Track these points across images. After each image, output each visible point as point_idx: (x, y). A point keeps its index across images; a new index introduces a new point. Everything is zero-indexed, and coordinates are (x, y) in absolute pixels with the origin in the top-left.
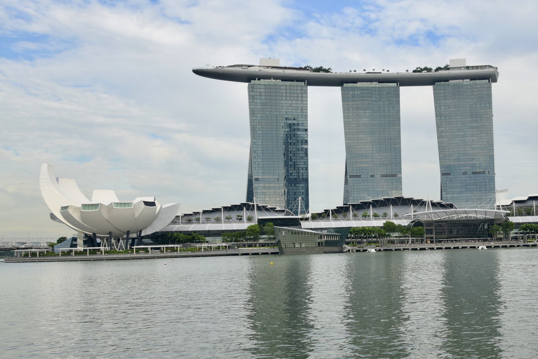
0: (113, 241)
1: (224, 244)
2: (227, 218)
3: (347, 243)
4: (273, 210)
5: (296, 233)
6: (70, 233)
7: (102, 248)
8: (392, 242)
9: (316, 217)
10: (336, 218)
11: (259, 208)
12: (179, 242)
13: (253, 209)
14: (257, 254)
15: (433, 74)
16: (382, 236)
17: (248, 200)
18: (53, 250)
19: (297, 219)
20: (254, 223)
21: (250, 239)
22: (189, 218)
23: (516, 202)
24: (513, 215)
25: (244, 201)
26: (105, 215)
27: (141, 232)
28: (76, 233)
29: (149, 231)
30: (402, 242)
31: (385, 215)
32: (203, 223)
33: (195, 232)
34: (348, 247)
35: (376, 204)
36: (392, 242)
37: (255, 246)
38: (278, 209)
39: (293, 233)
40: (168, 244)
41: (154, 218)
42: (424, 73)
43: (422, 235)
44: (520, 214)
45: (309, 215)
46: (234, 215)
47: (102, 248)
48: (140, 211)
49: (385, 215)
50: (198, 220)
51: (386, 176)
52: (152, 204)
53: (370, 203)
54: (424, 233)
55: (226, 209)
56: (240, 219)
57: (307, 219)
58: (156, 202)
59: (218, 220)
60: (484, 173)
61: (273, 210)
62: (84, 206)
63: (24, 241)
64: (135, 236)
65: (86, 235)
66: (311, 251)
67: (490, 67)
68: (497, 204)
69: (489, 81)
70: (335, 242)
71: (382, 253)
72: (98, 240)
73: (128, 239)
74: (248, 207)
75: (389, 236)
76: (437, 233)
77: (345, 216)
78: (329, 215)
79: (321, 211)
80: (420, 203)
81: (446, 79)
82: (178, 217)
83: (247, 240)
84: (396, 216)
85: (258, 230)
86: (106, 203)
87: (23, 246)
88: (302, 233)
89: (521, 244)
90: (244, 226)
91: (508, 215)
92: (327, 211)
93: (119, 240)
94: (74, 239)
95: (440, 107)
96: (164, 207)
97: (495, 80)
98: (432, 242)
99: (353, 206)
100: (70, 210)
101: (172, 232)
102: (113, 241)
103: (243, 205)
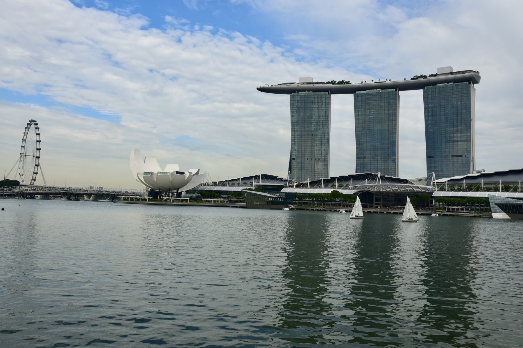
51: (385, 158)
69: (470, 83)
95: (428, 105)
97: (477, 83)
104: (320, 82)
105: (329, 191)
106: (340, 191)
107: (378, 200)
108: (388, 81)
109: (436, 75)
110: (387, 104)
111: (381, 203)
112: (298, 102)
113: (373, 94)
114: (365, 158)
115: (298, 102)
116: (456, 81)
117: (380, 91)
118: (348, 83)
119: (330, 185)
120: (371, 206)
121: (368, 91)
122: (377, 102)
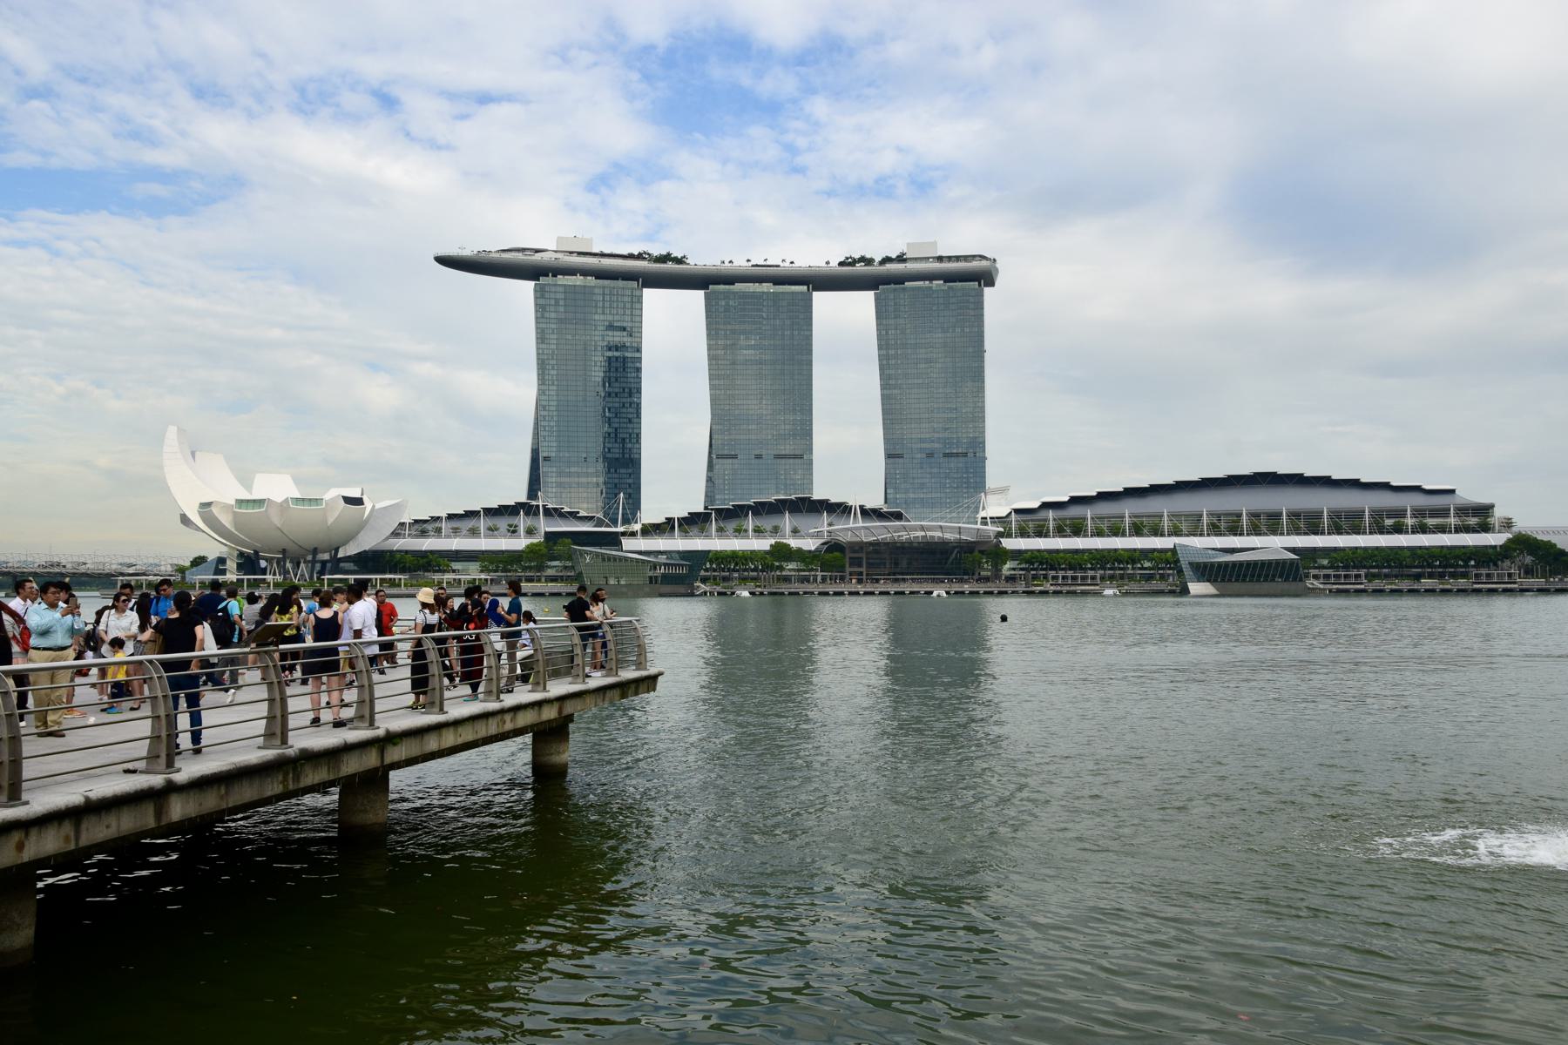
0: (289, 565)
1: (483, 576)
2: (490, 529)
3: (704, 580)
4: (574, 515)
5: (610, 558)
6: (213, 548)
7: (269, 577)
8: (787, 579)
9: (648, 530)
10: (685, 533)
11: (548, 512)
12: (403, 571)
13: (536, 514)
14: (541, 595)
15: (875, 269)
16: (768, 567)
17: (529, 497)
18: (183, 578)
19: (616, 533)
20: (538, 539)
21: (530, 568)
22: (422, 527)
23: (1017, 511)
24: (1009, 536)
25: (523, 498)
26: (276, 520)
27: (337, 550)
28: (225, 549)
29: (351, 550)
30: (805, 580)
31: (776, 530)
32: (447, 537)
33: (432, 552)
34: (703, 587)
35: (761, 509)
36: (787, 579)
37: (539, 581)
38: (583, 513)
39: (605, 558)
40: (384, 572)
41: (362, 525)
42: (860, 267)
43: (842, 568)
44: (1023, 533)
45: (637, 527)
46: (503, 523)
47: (269, 577)
48: (336, 514)
49: (776, 530)
50: (439, 530)
52: (358, 502)
53: (749, 507)
54: (847, 564)
55: (489, 512)
56: (513, 531)
57: (633, 534)
58: (365, 499)
59: (474, 532)
60: (965, 454)
61: (574, 515)
62: (240, 502)
63: (132, 561)
64: (326, 556)
65: (241, 554)
66: (636, 592)
67: (983, 257)
68: (982, 514)
70: (680, 577)
71: (768, 599)
72: (263, 564)
73: (314, 561)
74: (528, 509)
75: (781, 568)
76: (869, 565)
77: (702, 530)
78: (673, 528)
79: (660, 519)
80: (841, 509)
81: (899, 279)
82: (402, 524)
83: (524, 569)
84: (795, 532)
85: (545, 551)
86: (278, 497)
87: (131, 571)
88: (626, 559)
89: (1020, 589)
90: (520, 543)
91: (1000, 535)
92: (670, 520)
93: (298, 564)
94: (221, 561)
96: (378, 506)
98: (860, 581)
99: (718, 511)
100: (214, 509)
101: (392, 552)
102: (289, 565)
103: (520, 505)
104: (607, 251)
105: (763, 544)
106: (794, 543)
107: (856, 562)
108: (787, 264)
109: (901, 259)
110: (788, 322)
111: (863, 569)
112: (557, 304)
113: (753, 295)
114: (735, 457)
115: (557, 304)
116: (949, 278)
117: (767, 287)
118: (679, 261)
119: (731, 526)
120: (842, 579)
121: (739, 287)
122: (761, 313)
